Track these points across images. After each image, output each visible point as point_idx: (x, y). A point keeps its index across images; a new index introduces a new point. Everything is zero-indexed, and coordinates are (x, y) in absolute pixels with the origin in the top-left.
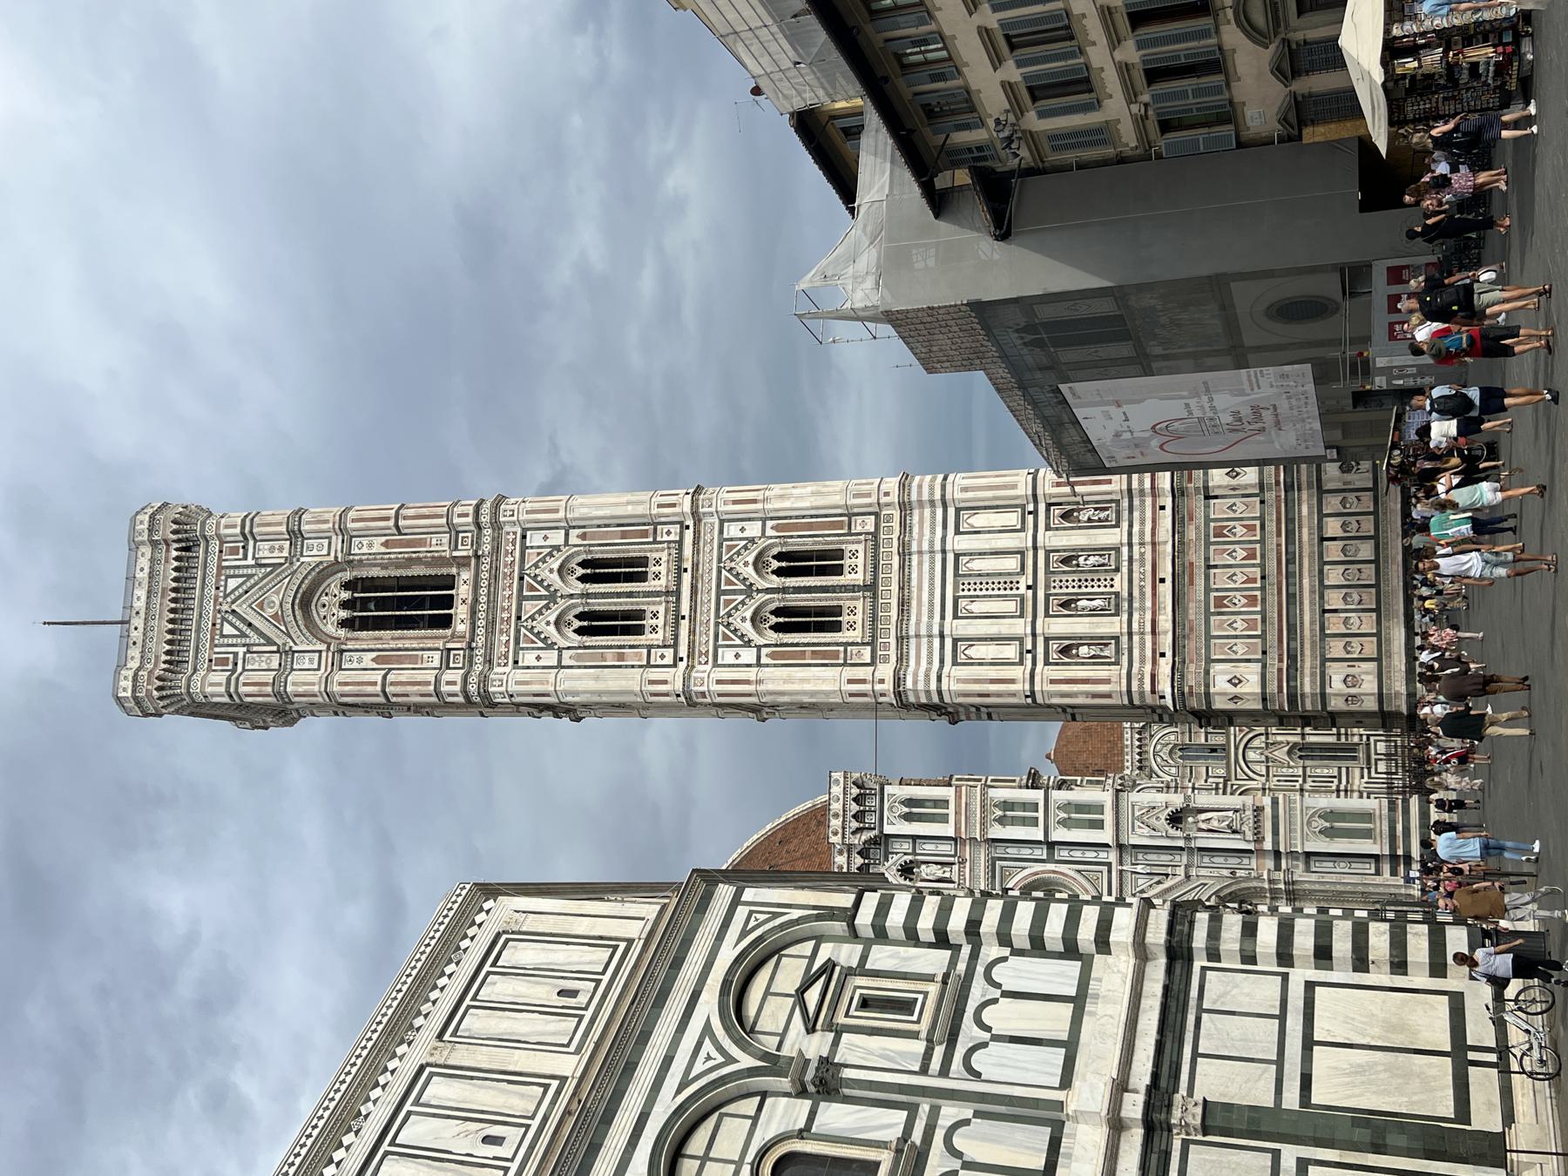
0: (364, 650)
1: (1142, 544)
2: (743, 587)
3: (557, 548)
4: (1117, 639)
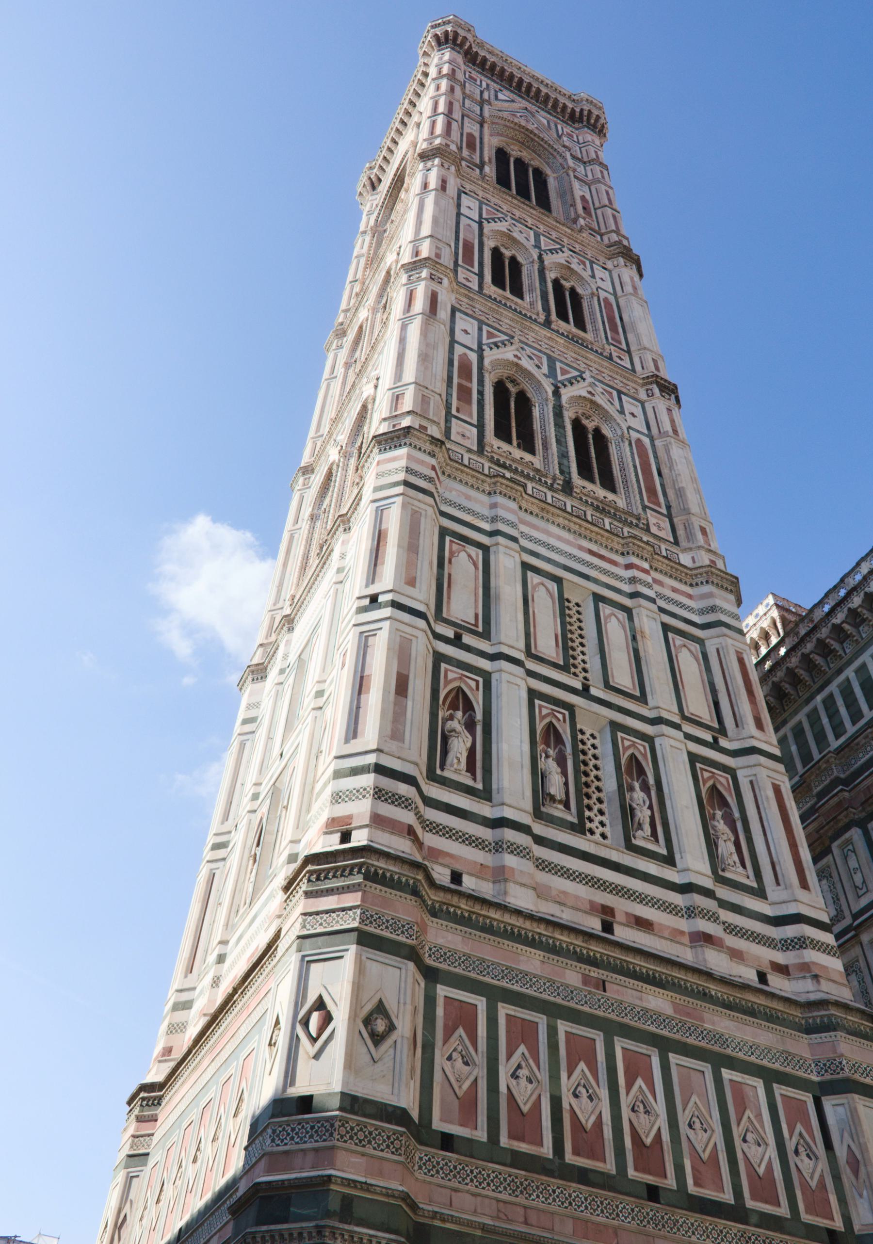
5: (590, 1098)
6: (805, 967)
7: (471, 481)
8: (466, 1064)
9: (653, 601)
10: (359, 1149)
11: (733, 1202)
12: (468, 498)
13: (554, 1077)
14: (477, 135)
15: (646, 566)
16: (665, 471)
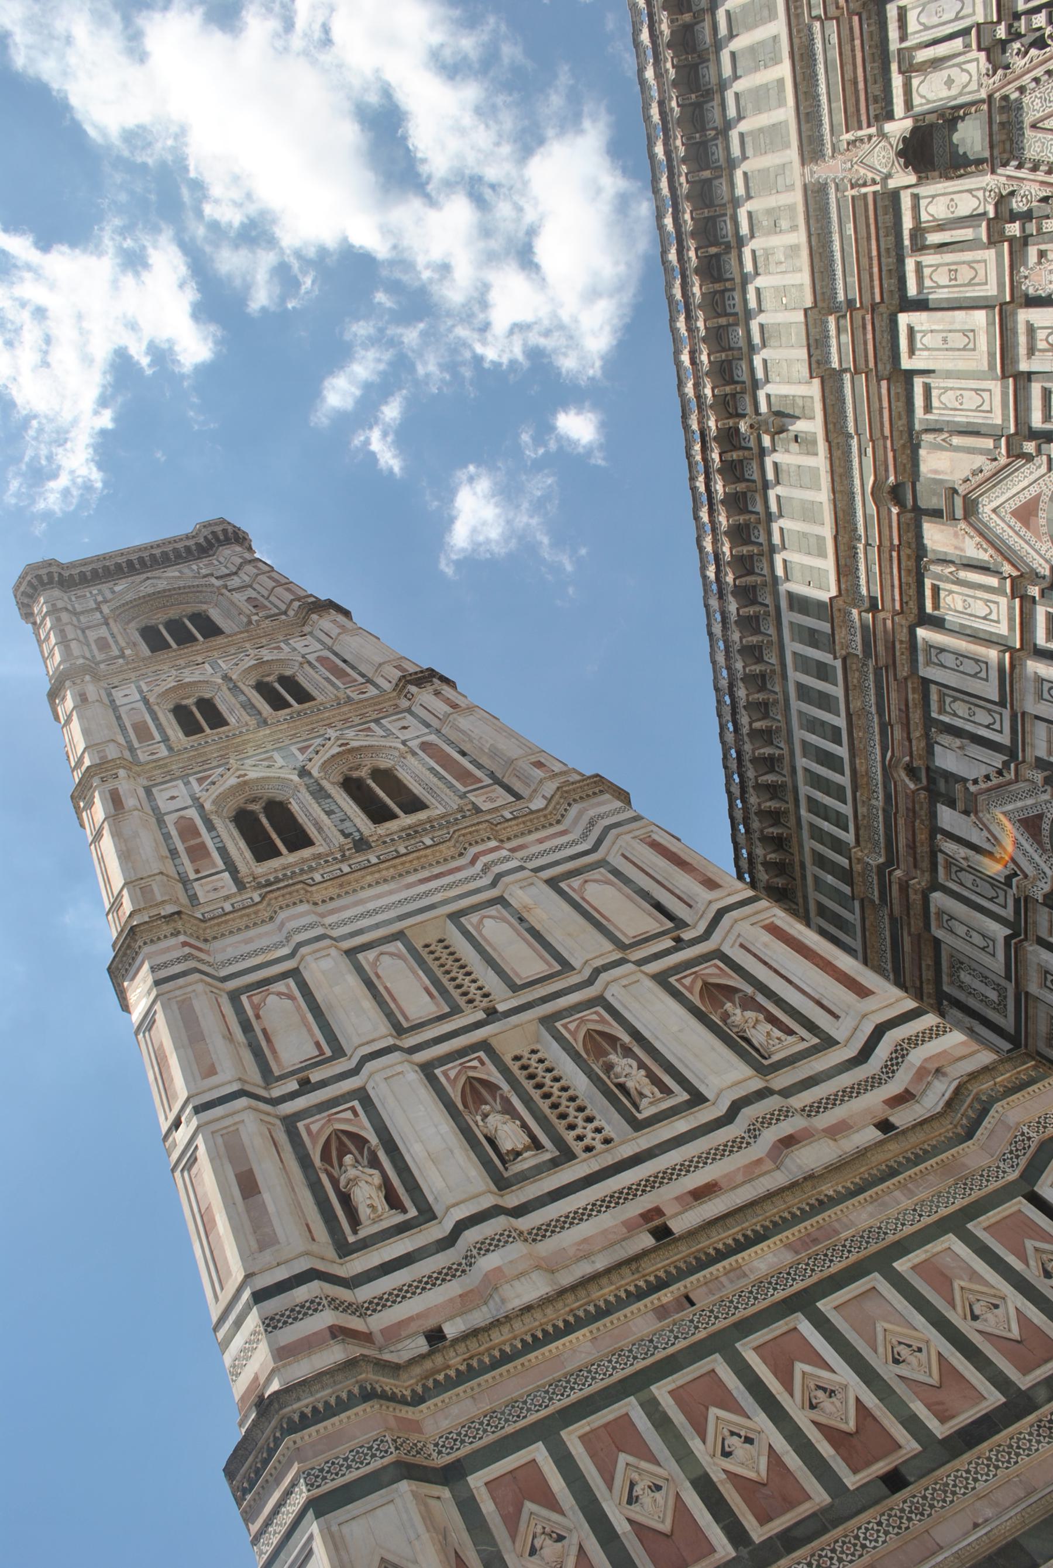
1: (753, 1132)
5: (749, 1440)
6: (922, 1073)
7: (242, 924)
8: (560, 1538)
9: (522, 868)
11: (1003, 1400)
15: (493, 844)
16: (466, 748)
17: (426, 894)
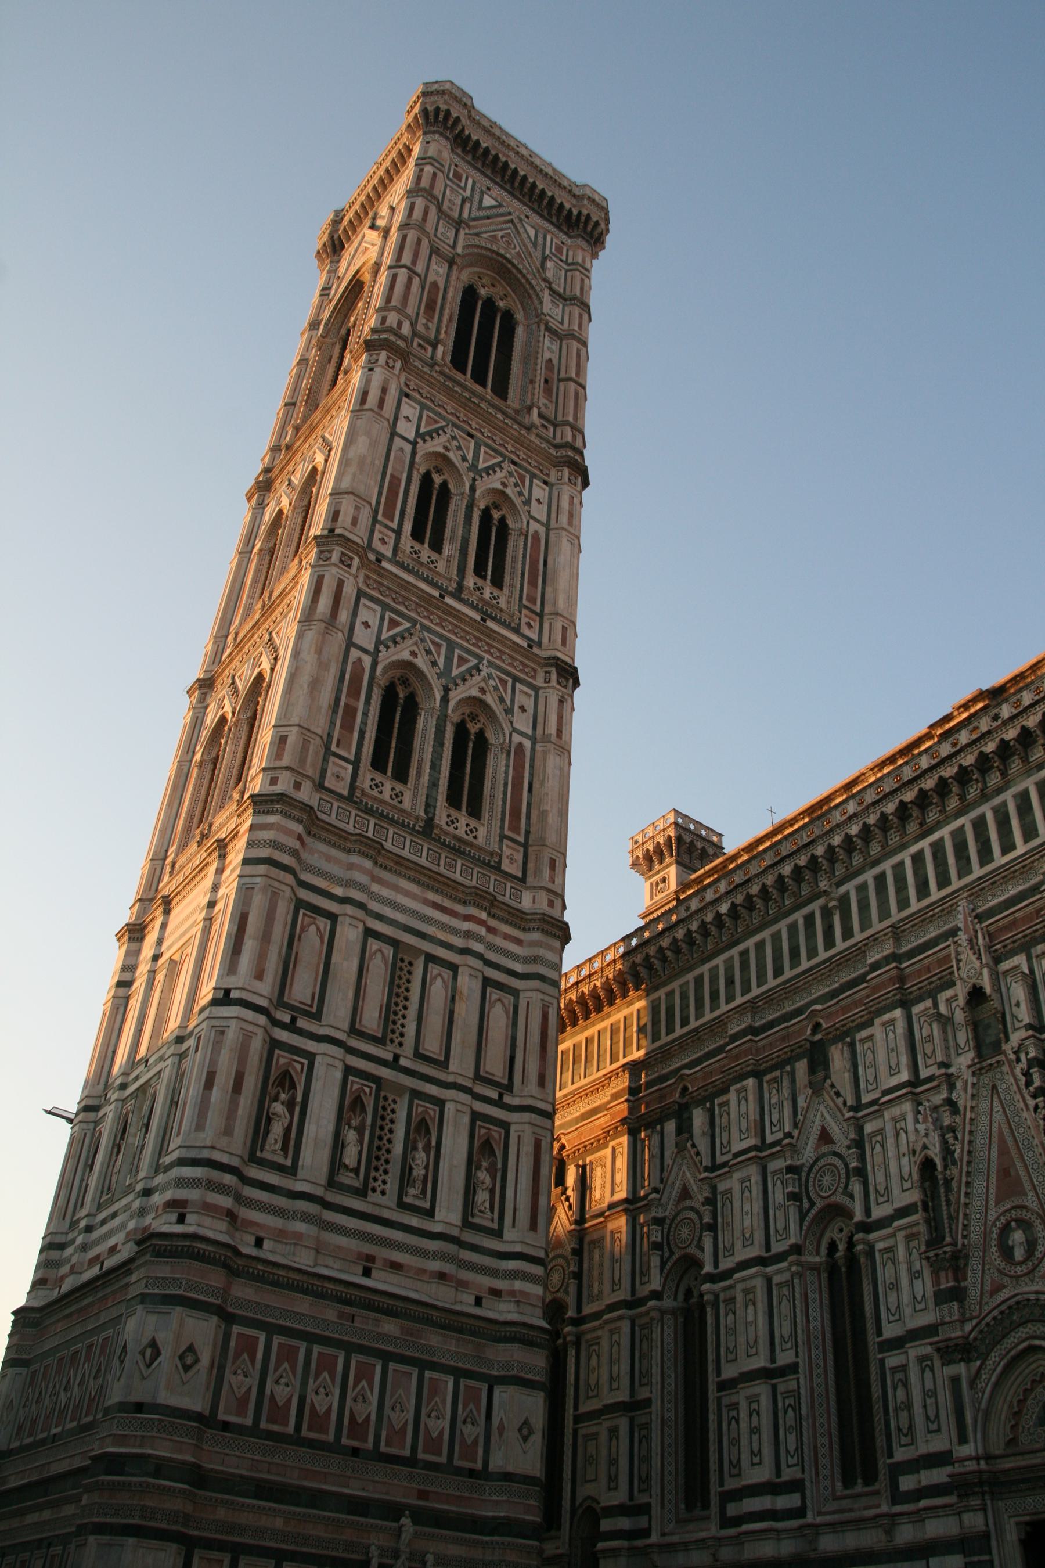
0: (447, 281)
2: (453, 675)
3: (528, 503)
4: (292, 1171)
5: (327, 1395)
6: (512, 1293)
10: (169, 1437)
12: (329, 859)
13: (304, 1383)
14: (441, 285)
15: (483, 915)
17: (429, 920)
